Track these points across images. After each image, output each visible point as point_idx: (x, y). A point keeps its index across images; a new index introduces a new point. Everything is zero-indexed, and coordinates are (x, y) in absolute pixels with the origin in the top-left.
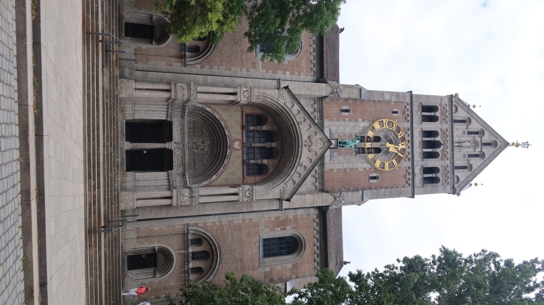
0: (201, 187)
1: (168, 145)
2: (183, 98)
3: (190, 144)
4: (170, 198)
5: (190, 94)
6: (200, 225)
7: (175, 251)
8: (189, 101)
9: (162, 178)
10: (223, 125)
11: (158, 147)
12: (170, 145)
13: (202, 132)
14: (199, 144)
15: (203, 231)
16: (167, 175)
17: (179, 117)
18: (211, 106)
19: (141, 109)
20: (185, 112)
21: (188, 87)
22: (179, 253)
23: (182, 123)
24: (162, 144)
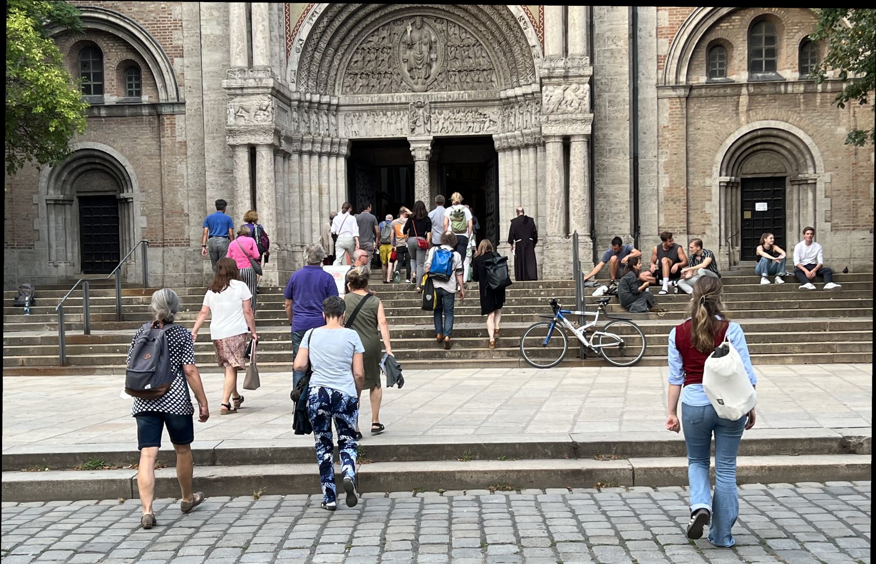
0: (543, 48)
1: (421, 152)
2: (270, 109)
3: (416, 87)
4: (566, 141)
5: (258, 87)
6: (664, 50)
7: (739, 125)
8: (278, 91)
9: (517, 167)
11: (427, 180)
12: (420, 145)
13: (377, 50)
14: (416, 59)
15: (685, 37)
17: (337, 120)
20: (319, 103)
21: (236, 95)
22: (748, 111)
24: (417, 169)
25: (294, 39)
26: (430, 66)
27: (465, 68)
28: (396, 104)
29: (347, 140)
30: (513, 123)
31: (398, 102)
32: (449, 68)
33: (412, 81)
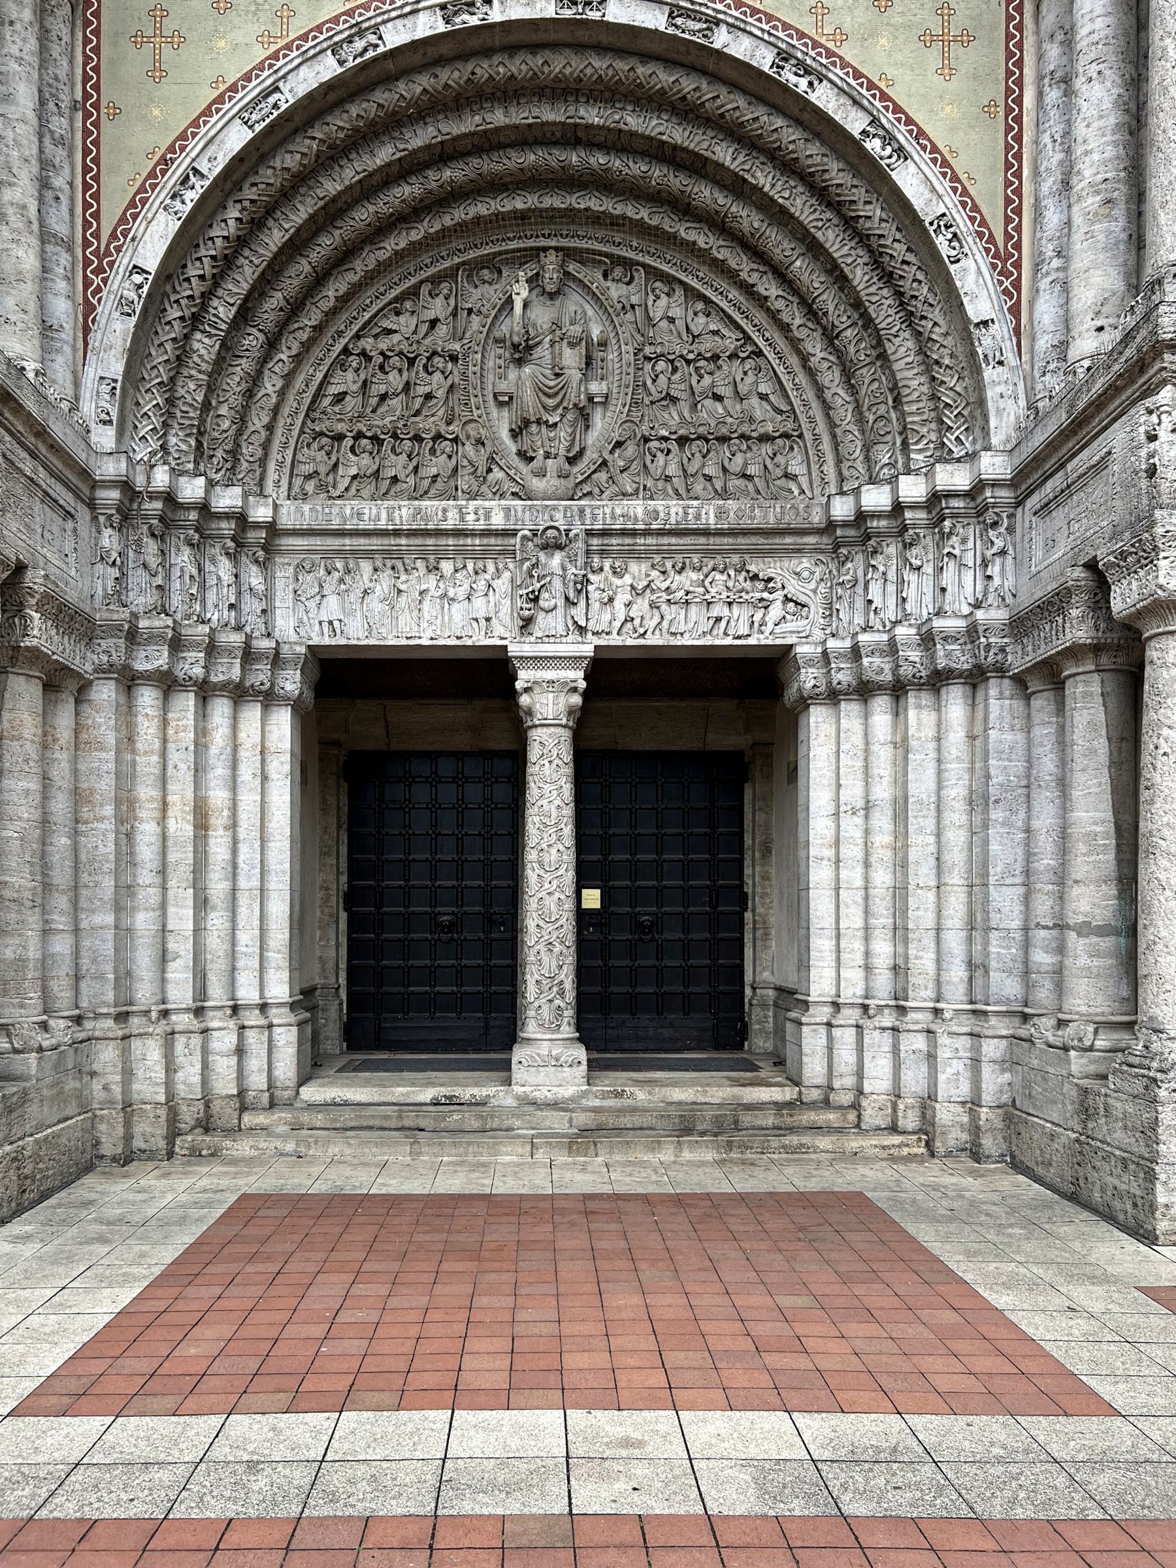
3: (537, 484)
9: (883, 756)
10: (328, 69)
11: (568, 790)
12: (550, 674)
13: (411, 362)
14: (542, 391)
16: (850, 710)
17: (269, 580)
18: (111, 210)
19: (181, 947)
23: (329, 554)
24: (534, 753)
25: (111, 264)
26: (584, 416)
27: (701, 430)
28: (472, 534)
29: (302, 650)
30: (878, 602)
31: (481, 525)
32: (645, 429)
33: (524, 469)
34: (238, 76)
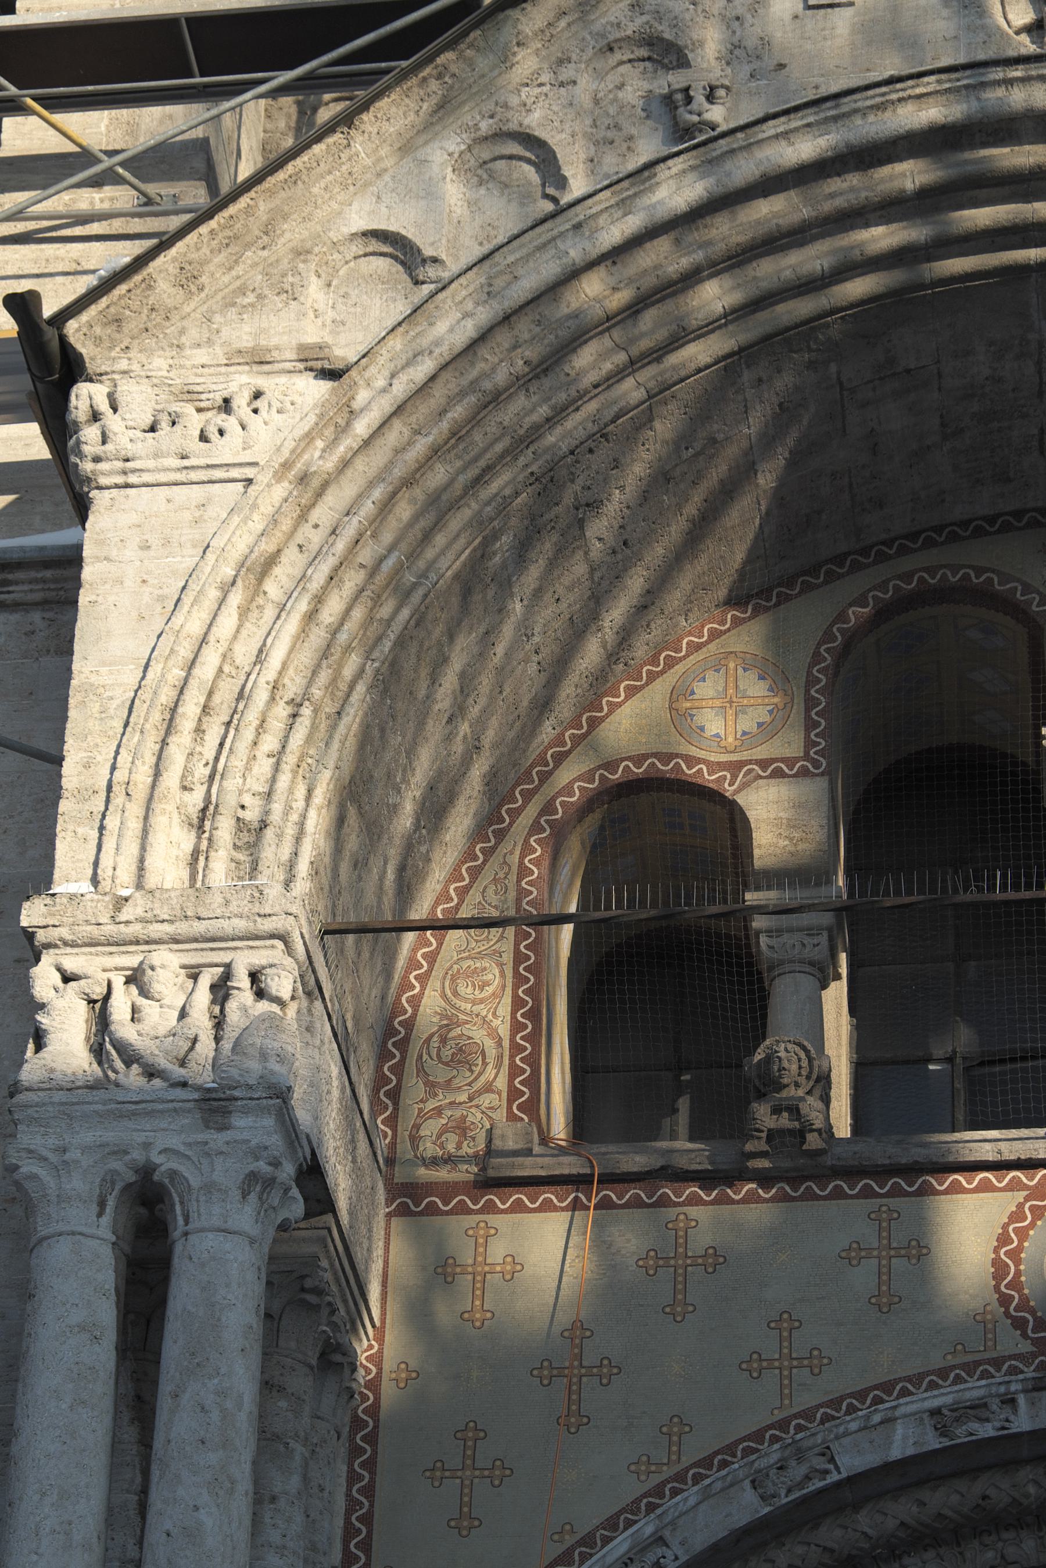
34: (596, 1522)
